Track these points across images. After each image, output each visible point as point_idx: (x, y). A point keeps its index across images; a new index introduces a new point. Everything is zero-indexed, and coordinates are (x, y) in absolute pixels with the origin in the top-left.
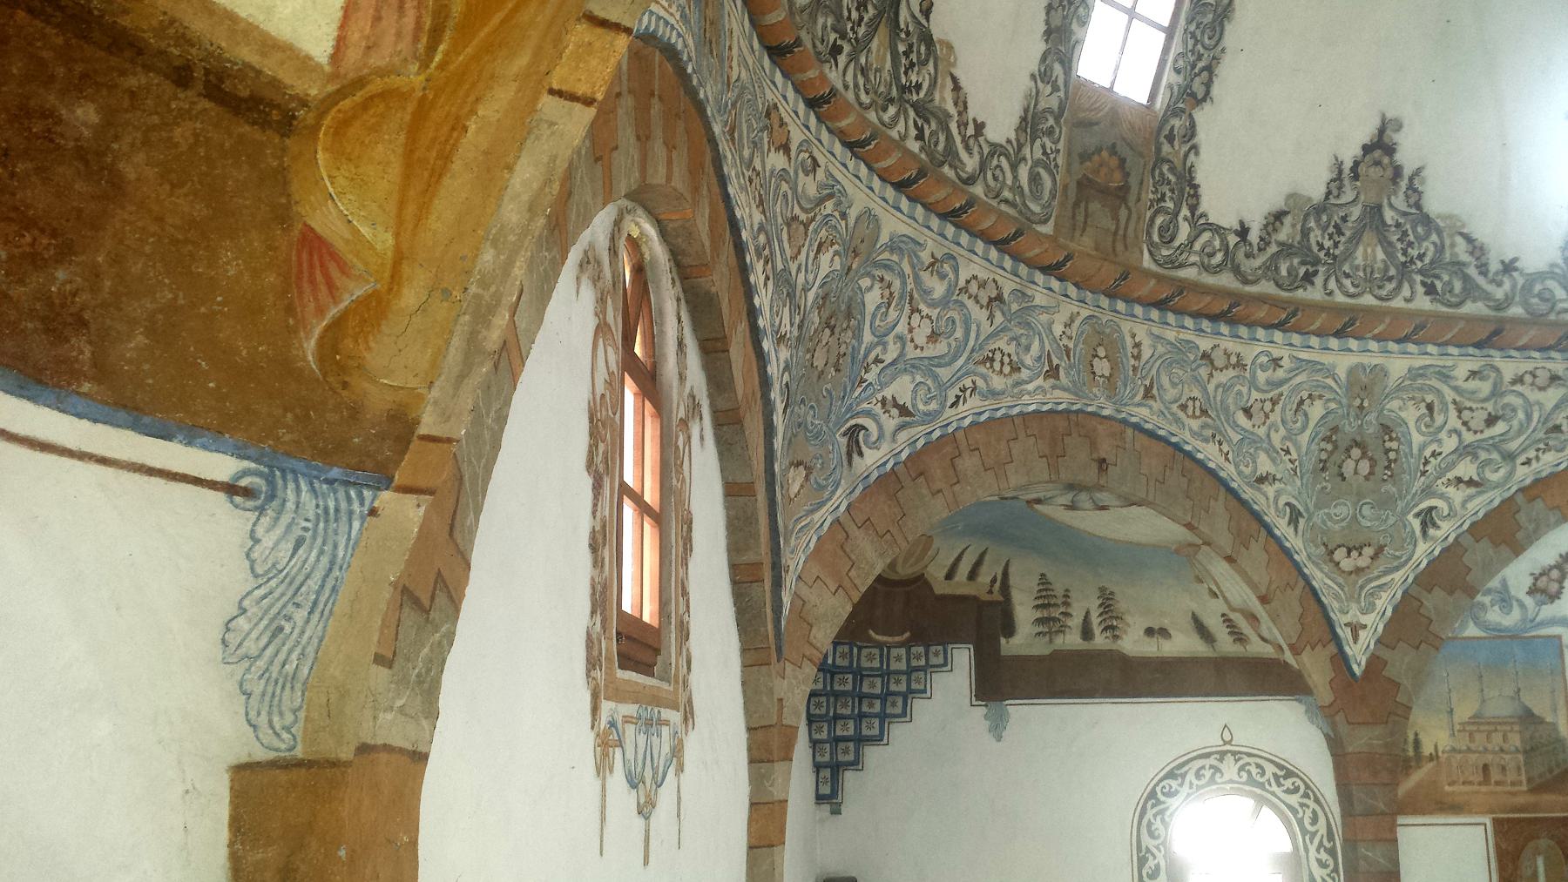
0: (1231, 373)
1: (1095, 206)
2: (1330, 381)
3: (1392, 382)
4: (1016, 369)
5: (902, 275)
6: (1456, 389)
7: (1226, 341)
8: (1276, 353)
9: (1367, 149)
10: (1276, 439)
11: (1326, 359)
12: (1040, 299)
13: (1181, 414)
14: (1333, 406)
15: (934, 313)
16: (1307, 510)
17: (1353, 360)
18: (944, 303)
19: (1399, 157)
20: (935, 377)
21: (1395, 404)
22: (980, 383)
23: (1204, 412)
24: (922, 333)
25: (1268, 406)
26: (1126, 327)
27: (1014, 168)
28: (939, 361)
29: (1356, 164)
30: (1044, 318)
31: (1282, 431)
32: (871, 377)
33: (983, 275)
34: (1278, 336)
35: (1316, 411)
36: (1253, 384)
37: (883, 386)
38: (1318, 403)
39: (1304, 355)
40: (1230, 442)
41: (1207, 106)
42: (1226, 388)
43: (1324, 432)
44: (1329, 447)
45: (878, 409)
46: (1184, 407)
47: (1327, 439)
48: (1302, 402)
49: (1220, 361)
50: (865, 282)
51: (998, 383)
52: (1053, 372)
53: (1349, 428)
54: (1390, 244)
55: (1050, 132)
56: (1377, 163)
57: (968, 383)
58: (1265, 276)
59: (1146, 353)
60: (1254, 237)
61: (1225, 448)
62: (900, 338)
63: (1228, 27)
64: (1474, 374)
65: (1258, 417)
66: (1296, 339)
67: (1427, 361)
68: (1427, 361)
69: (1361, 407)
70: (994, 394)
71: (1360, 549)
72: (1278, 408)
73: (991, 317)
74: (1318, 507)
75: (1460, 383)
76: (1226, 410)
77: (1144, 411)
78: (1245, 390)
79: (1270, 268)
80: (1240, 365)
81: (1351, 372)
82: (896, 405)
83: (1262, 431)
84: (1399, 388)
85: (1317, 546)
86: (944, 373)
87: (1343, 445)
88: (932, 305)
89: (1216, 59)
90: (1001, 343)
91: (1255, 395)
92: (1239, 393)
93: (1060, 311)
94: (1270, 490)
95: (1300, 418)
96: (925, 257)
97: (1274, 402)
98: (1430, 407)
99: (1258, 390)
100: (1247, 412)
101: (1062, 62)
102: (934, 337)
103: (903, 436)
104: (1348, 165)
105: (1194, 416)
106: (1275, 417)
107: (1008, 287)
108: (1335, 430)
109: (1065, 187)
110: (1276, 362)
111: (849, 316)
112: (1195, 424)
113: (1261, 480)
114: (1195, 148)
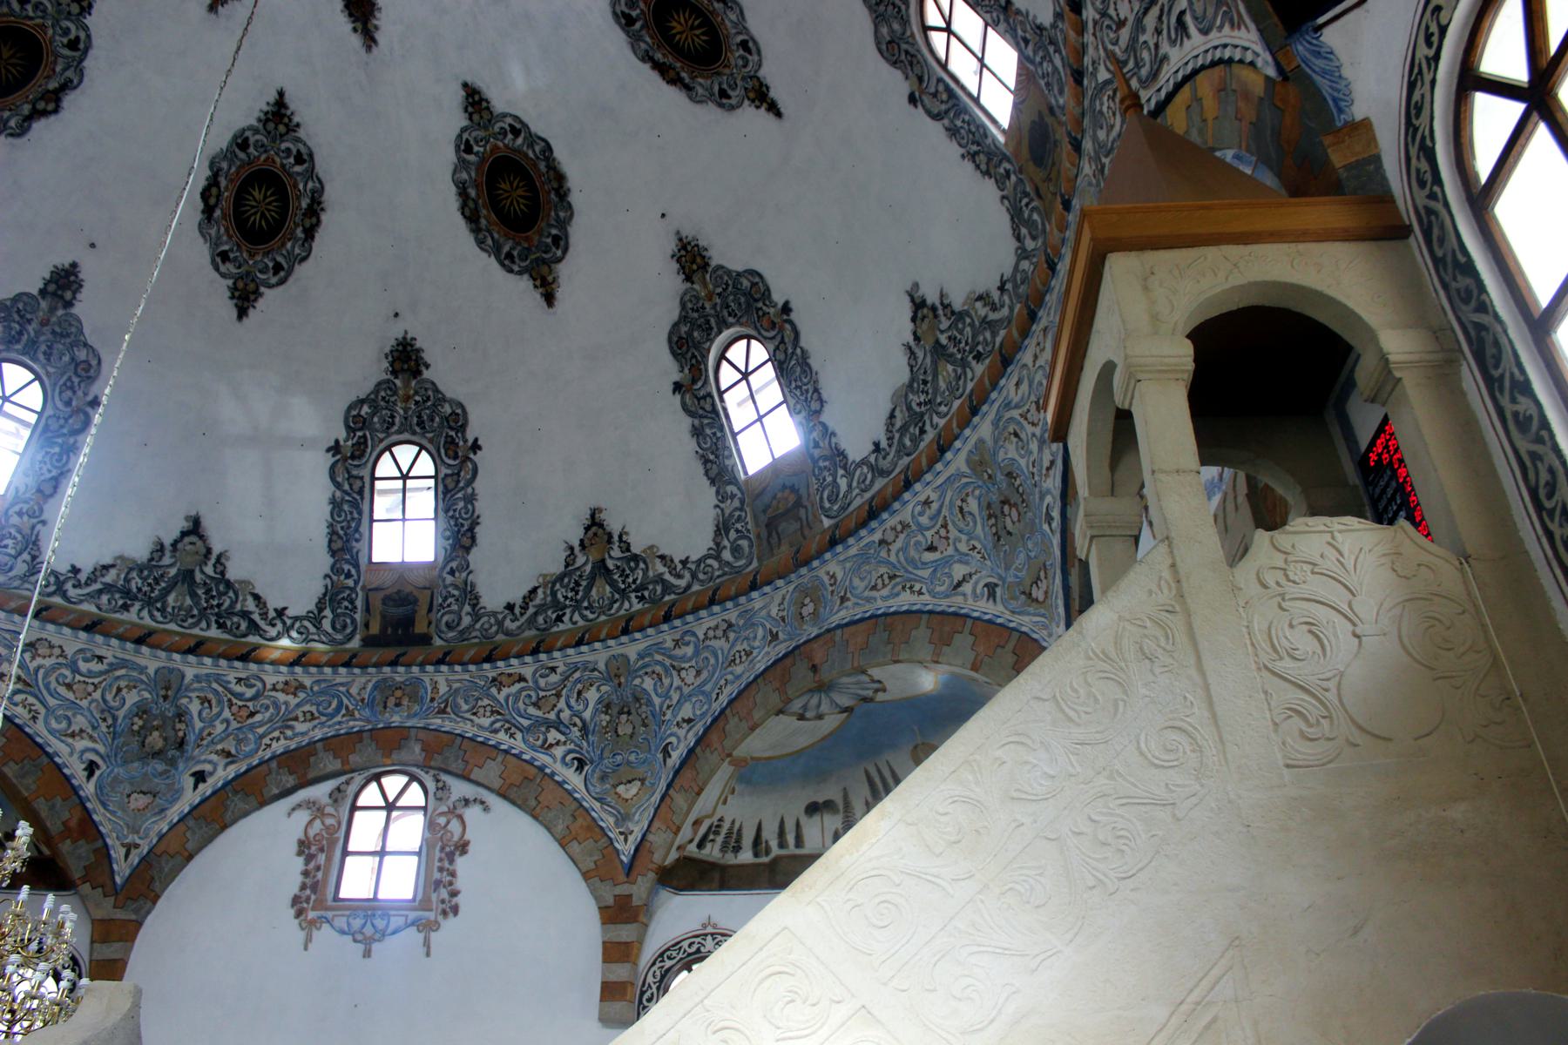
0: (902, 536)
1: (782, 526)
2: (965, 480)
3: (990, 443)
4: (748, 654)
5: (658, 663)
6: (1017, 407)
7: (889, 520)
8: (922, 498)
9: (914, 319)
10: (963, 548)
11: (952, 470)
12: (757, 605)
13: (874, 593)
14: (977, 492)
15: (693, 663)
16: (1000, 577)
17: (963, 455)
18: (697, 653)
19: (929, 302)
20: (703, 693)
21: (1001, 455)
22: (730, 677)
23: (891, 578)
24: (690, 677)
25: (943, 532)
26: (822, 573)
27: (718, 558)
28: (704, 683)
29: (915, 333)
30: (764, 613)
31: (964, 537)
32: (668, 717)
33: (712, 624)
34: (918, 486)
35: (973, 505)
36: (922, 529)
37: (675, 717)
38: (970, 499)
39: (940, 481)
40: (920, 580)
41: (826, 408)
42: (904, 549)
43: (985, 513)
44: (993, 521)
45: (675, 729)
46: (874, 588)
47: (990, 516)
48: (961, 509)
49: (890, 536)
50: (637, 681)
51: (739, 669)
52: (775, 637)
53: (995, 498)
54: (952, 355)
55: (739, 519)
56: (924, 318)
57: (722, 682)
58: (900, 458)
59: (839, 576)
60: (884, 444)
61: (917, 588)
62: (678, 688)
63: (810, 361)
64: (1017, 384)
65: (941, 545)
66: (928, 477)
67: (996, 405)
68: (996, 405)
69: (990, 477)
70: (738, 677)
71: (1039, 578)
72: (950, 527)
73: (727, 639)
74: (1007, 568)
75: (1016, 400)
76: (912, 562)
77: (842, 613)
78: (920, 538)
79: (902, 451)
80: (905, 526)
81: (968, 462)
82: (684, 720)
83: (950, 551)
84: (996, 442)
85: (1014, 598)
86: (707, 688)
87: (998, 513)
88: (690, 659)
89: (816, 382)
90: (739, 647)
91: (928, 534)
92: (918, 543)
93: (769, 603)
94: (967, 588)
95: (969, 519)
96: (669, 644)
97: (945, 526)
98: (1016, 435)
99: (928, 529)
100: (931, 548)
101: (730, 483)
102: (698, 673)
103: (691, 733)
104: (910, 339)
105: (884, 585)
106: (953, 533)
107: (732, 616)
108: (989, 506)
109: (758, 536)
110: (927, 503)
111: (637, 700)
112: (885, 592)
113: (959, 584)
114: (833, 434)
